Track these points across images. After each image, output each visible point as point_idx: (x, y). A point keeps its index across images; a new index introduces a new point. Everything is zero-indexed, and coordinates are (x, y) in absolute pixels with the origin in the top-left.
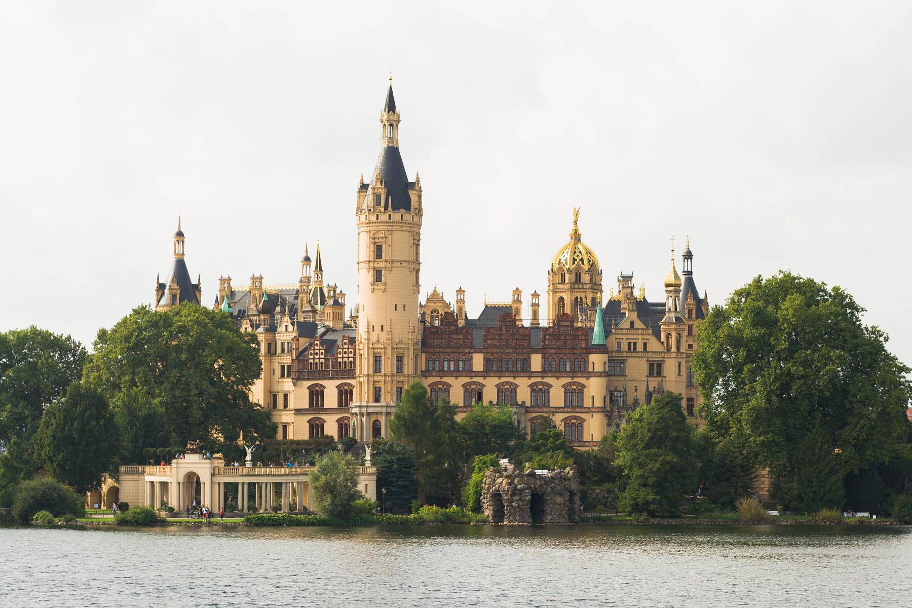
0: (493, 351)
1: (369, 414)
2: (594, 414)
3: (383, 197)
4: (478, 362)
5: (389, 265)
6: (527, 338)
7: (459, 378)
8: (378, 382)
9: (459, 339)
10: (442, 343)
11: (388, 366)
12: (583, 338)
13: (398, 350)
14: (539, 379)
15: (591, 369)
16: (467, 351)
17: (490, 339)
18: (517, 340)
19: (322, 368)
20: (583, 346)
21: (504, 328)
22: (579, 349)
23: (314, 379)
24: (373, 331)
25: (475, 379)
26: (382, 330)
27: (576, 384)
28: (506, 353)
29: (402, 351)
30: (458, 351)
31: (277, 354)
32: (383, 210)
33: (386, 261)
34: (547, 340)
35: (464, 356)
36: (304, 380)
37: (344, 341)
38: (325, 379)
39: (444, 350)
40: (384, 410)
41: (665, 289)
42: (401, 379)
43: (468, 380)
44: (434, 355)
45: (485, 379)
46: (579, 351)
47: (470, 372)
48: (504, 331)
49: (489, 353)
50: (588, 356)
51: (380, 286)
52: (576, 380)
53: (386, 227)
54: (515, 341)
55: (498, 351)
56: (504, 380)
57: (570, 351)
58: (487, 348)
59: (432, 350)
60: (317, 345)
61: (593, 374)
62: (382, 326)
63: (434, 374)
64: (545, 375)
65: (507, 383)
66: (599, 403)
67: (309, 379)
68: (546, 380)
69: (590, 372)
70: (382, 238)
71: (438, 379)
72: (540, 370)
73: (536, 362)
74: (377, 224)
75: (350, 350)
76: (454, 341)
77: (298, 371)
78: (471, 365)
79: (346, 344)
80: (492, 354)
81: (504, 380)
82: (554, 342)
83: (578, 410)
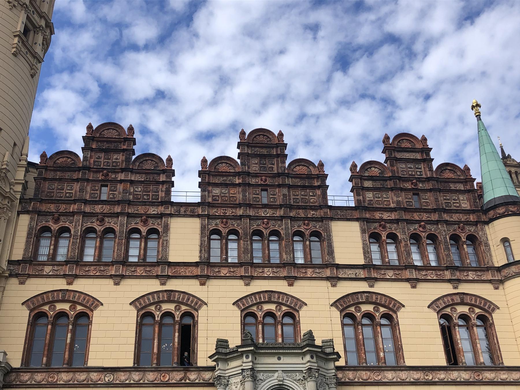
6: (316, 183)
9: (132, 182)
12: (461, 187)
14: (362, 287)
16: (153, 210)
17: (216, 185)
18: (289, 187)
22: (457, 211)
25: (174, 285)
27: (468, 300)
28: (263, 218)
34: (368, 189)
45: (203, 284)
46: (455, 217)
49: (215, 217)
50: (482, 230)
52: (464, 288)
54: (285, 191)
56: (258, 286)
57: (435, 217)
59: (52, 208)
64: (374, 275)
68: (381, 288)
69: (499, 269)
76: (120, 187)
78: (165, 246)
81: (258, 286)
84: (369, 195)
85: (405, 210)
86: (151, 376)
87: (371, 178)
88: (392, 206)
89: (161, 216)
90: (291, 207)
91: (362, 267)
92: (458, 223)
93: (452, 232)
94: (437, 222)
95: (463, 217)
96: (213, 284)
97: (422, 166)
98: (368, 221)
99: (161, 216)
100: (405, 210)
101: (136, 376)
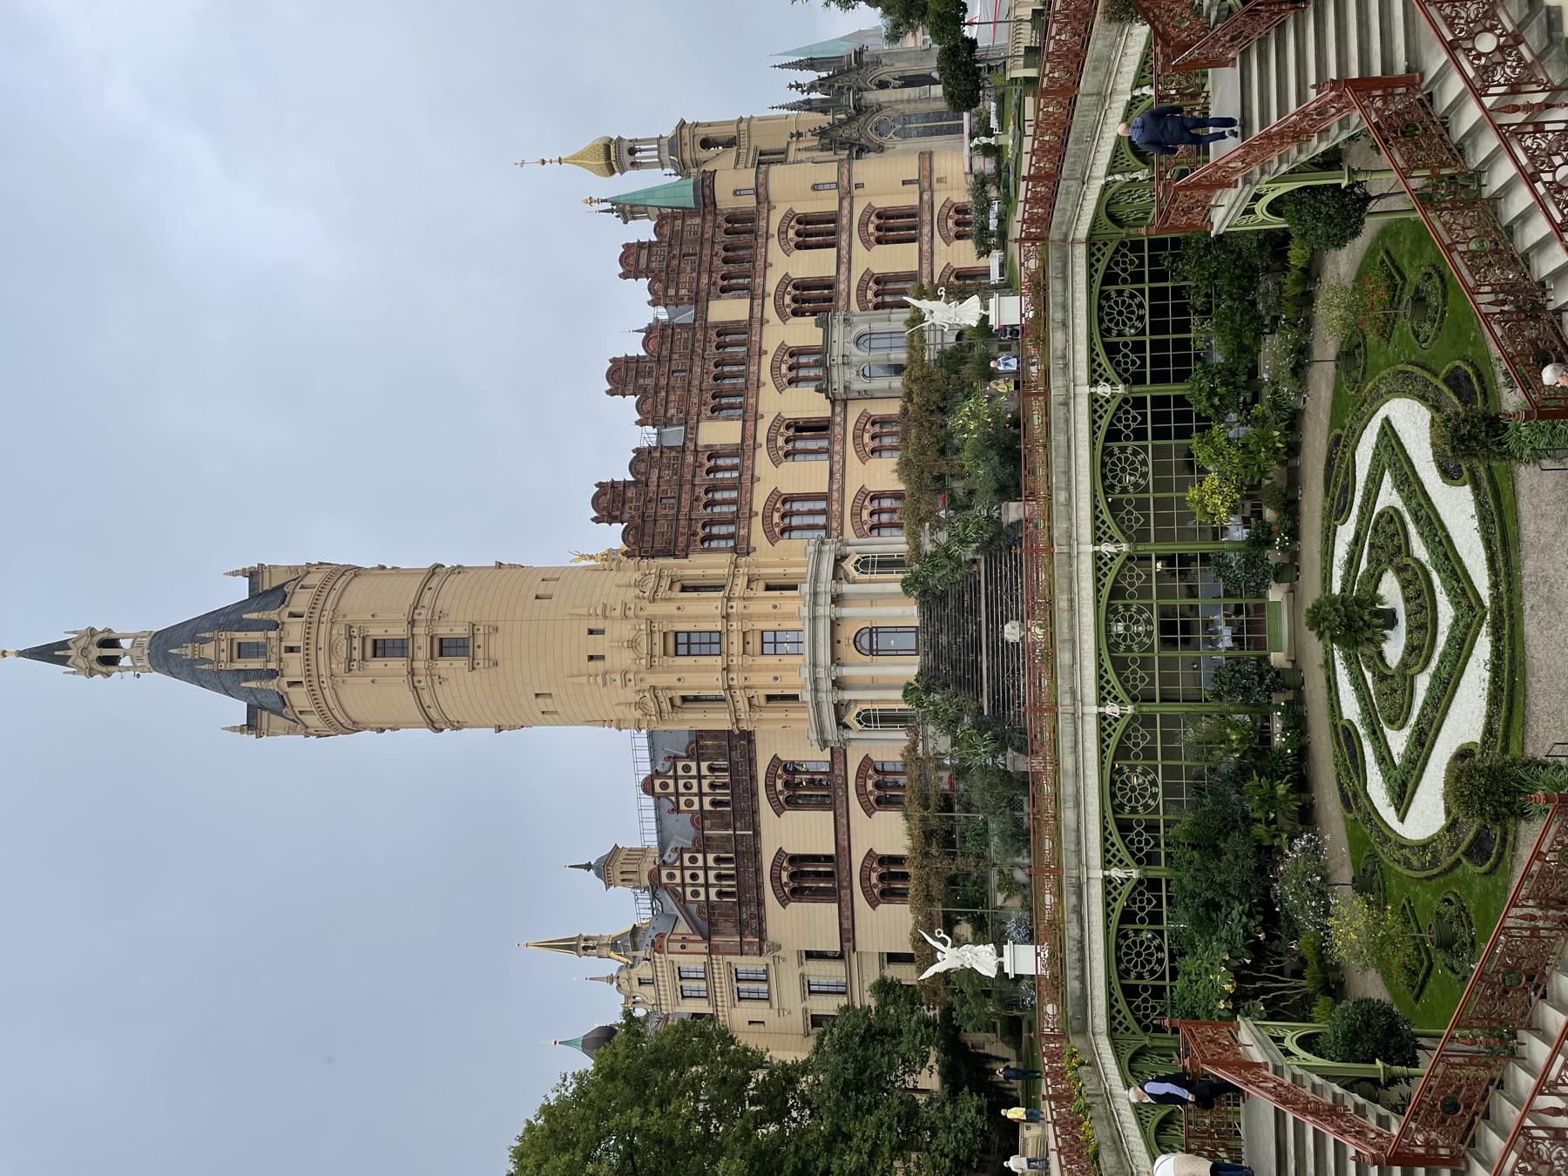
0: (696, 400)
1: (836, 660)
2: (855, 180)
3: (240, 636)
4: (719, 432)
5: (423, 614)
6: (670, 331)
7: (757, 473)
8: (746, 643)
9: (659, 477)
10: (666, 516)
11: (702, 612)
13: (661, 589)
14: (769, 302)
15: (749, 202)
16: (690, 459)
17: (666, 411)
18: (671, 352)
19: (728, 860)
20: (698, 220)
21: (641, 381)
22: (703, 227)
23: (759, 887)
24: (602, 658)
25: (762, 437)
26: (602, 632)
27: (784, 229)
29: (665, 583)
30: (689, 478)
31: (710, 1011)
32: (273, 634)
33: (412, 623)
34: (677, 293)
35: (701, 465)
36: (761, 919)
37: (658, 789)
38: (757, 853)
39: (685, 510)
40: (825, 609)
41: (617, 174)
42: (741, 582)
43: (762, 456)
44: (695, 534)
45: (762, 417)
47: (743, 450)
48: (650, 382)
51: (480, 640)
52: (774, 229)
53: (323, 627)
54: (675, 356)
55: (695, 391)
56: (766, 375)
57: (707, 246)
58: (688, 413)
59: (682, 540)
60: (671, 876)
61: (761, 190)
62: (591, 632)
63: (743, 532)
64: (760, 291)
65: (774, 369)
66: (829, 173)
67: (760, 903)
68: (771, 287)
69: (758, 203)
70: (350, 638)
71: (757, 523)
72: (748, 301)
73: (728, 310)
74: (312, 652)
75: (680, 772)
77: (741, 935)
79: (664, 786)
80: (700, 404)
81: (766, 375)
82: (684, 278)
83: (845, 221)
84: (683, 292)
85: (700, 264)
86: (837, 448)
87: (666, 289)
88: (695, 275)
89: (696, 452)
90: (693, 351)
91: (752, 299)
92: (714, 227)
93: (723, 234)
94: (713, 242)
95: (709, 224)
96: (761, 410)
97: (654, 249)
98: (708, 294)
99: (696, 452)
100: (700, 264)
101: (837, 458)
